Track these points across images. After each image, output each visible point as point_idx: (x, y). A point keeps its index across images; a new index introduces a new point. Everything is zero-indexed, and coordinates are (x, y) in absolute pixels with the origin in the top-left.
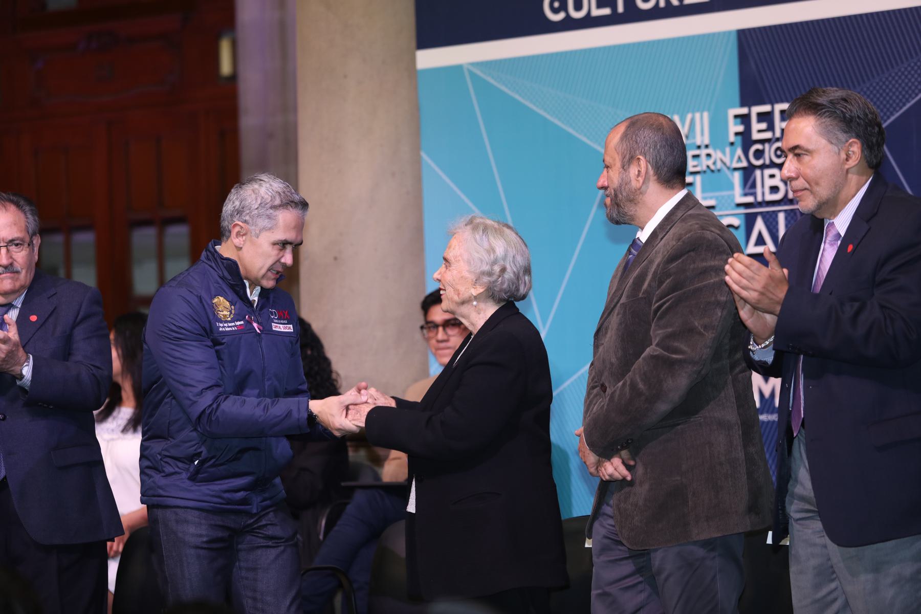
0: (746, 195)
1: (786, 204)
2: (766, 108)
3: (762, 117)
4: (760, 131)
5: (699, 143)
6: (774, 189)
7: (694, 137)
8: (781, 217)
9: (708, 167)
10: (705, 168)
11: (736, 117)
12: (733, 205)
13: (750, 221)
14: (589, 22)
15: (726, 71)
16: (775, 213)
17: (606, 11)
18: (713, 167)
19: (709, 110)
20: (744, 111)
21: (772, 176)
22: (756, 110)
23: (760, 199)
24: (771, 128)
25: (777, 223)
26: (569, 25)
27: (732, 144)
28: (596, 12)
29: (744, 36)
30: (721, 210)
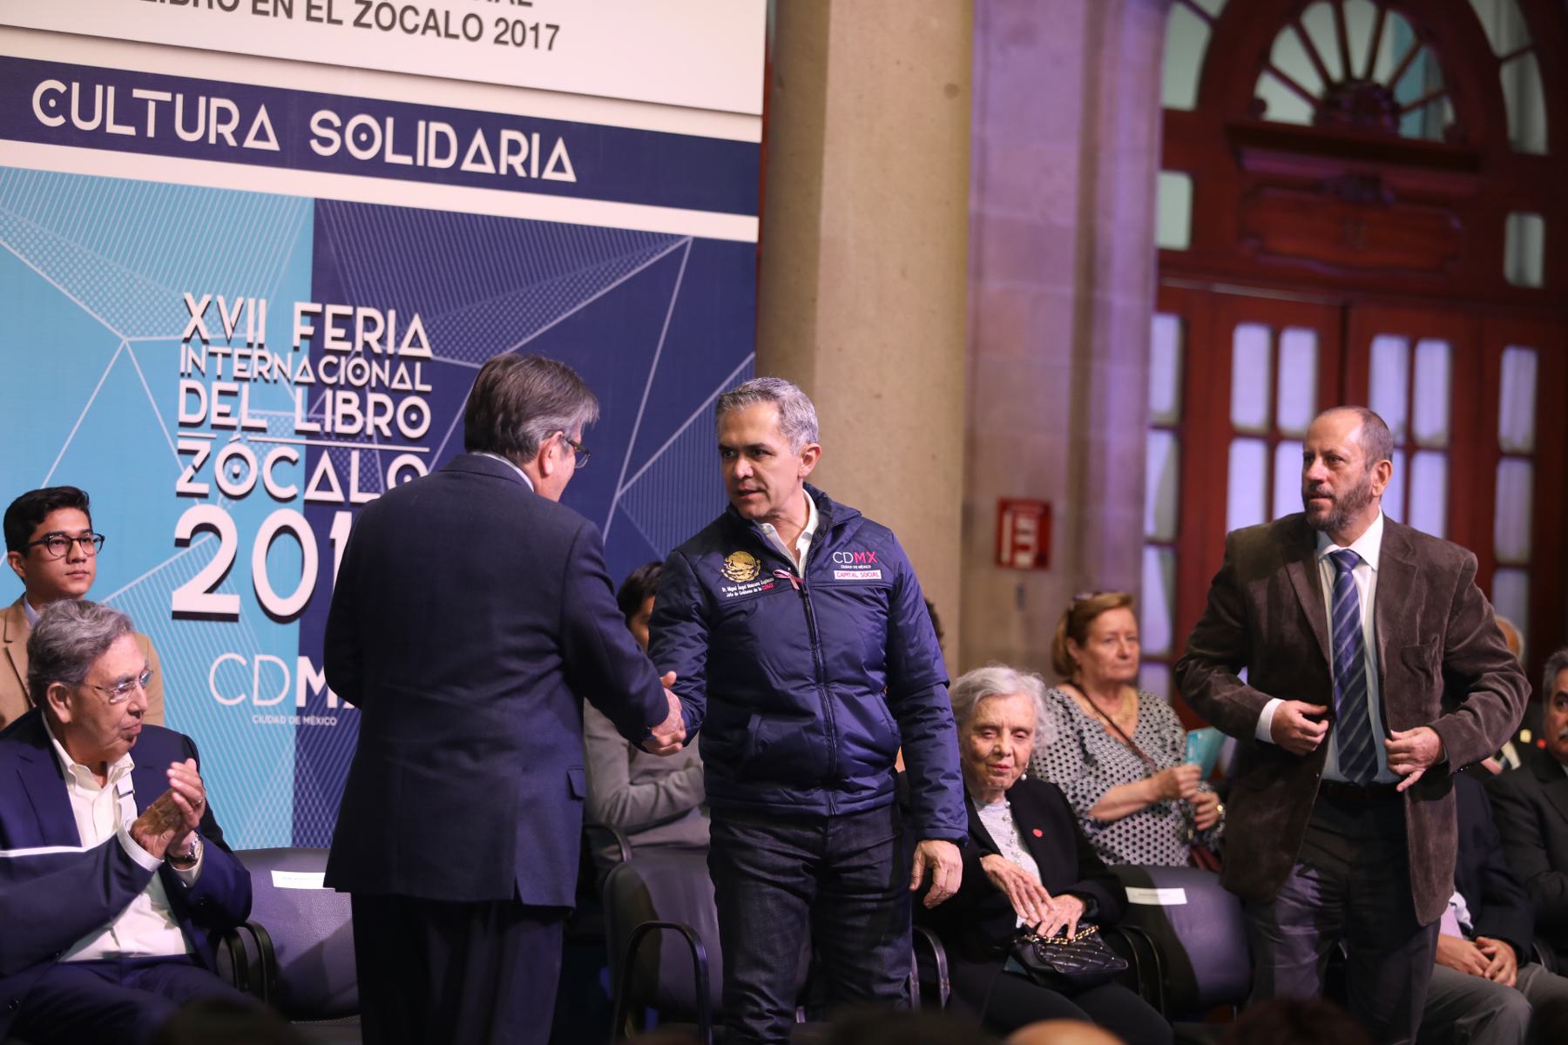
0: (309, 420)
1: (362, 441)
2: (347, 310)
3: (339, 320)
4: (334, 339)
5: (250, 340)
6: (348, 419)
7: (245, 331)
8: (355, 456)
10: (256, 375)
11: (304, 313)
12: (291, 431)
14: (100, 140)
15: (295, 252)
16: (348, 451)
17: (130, 131)
18: (267, 376)
19: (267, 298)
20: (317, 308)
22: (332, 309)
23: (328, 428)
24: (350, 337)
25: (349, 464)
26: (67, 136)
27: (296, 349)
28: (112, 128)
29: (325, 210)
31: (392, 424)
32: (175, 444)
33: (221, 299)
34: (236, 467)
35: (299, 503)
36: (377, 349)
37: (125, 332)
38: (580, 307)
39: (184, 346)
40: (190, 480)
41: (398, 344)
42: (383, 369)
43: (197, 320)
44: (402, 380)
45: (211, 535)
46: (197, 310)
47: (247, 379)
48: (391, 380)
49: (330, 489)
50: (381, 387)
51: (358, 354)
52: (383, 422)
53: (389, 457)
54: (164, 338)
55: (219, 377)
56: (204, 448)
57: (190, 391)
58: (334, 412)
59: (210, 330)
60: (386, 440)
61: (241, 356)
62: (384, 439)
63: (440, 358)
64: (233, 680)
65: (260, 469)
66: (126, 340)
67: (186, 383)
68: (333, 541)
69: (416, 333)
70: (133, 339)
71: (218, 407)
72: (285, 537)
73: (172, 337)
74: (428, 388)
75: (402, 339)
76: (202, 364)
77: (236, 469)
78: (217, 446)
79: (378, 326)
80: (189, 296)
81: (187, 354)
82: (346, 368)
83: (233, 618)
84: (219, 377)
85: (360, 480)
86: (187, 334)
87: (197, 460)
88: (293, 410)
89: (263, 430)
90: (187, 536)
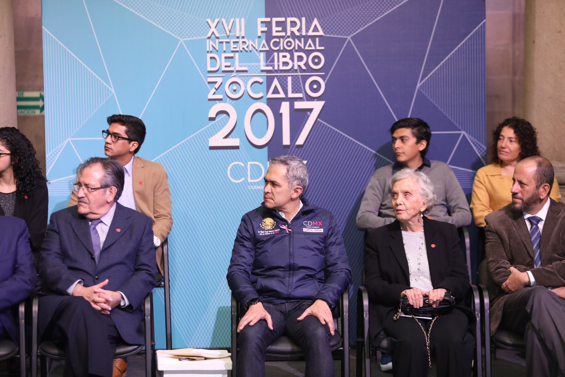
0: (267, 66)
1: (292, 72)
2: (283, 19)
3: (278, 24)
4: (277, 31)
5: (238, 35)
6: (285, 64)
7: (235, 32)
8: (290, 79)
9: (243, 48)
10: (241, 49)
11: (262, 22)
12: (259, 70)
13: (269, 81)
16: (286, 77)
18: (246, 49)
20: (268, 19)
21: (284, 57)
22: (275, 20)
23: (276, 68)
24: (284, 30)
27: (259, 37)
30: (251, 73)
31: (306, 64)
32: (207, 80)
33: (224, 20)
34: (235, 87)
35: (264, 99)
36: (297, 34)
37: (181, 37)
38: (395, 8)
39: (208, 40)
40: (214, 94)
41: (307, 31)
42: (300, 42)
43: (213, 29)
44: (310, 46)
45: (225, 115)
46: (213, 25)
47: (237, 51)
48: (305, 46)
49: (279, 93)
50: (300, 49)
51: (288, 37)
52: (302, 64)
53: (305, 78)
54: (199, 38)
55: (225, 52)
56: (219, 80)
58: (278, 62)
59: (219, 33)
60: (304, 71)
61: (234, 42)
62: (304, 71)
63: (328, 35)
64: (238, 172)
65: (246, 86)
66: (182, 40)
67: (209, 55)
68: (281, 114)
69: (316, 25)
70: (184, 40)
71: (224, 63)
72: (259, 114)
73: (202, 37)
74: (323, 48)
75: (309, 29)
77: (235, 88)
79: (297, 25)
81: (209, 45)
82: (283, 44)
83: (237, 148)
85: (292, 88)
86: (209, 35)
87: (217, 86)
88: (260, 62)
89: (246, 71)
90: (214, 116)
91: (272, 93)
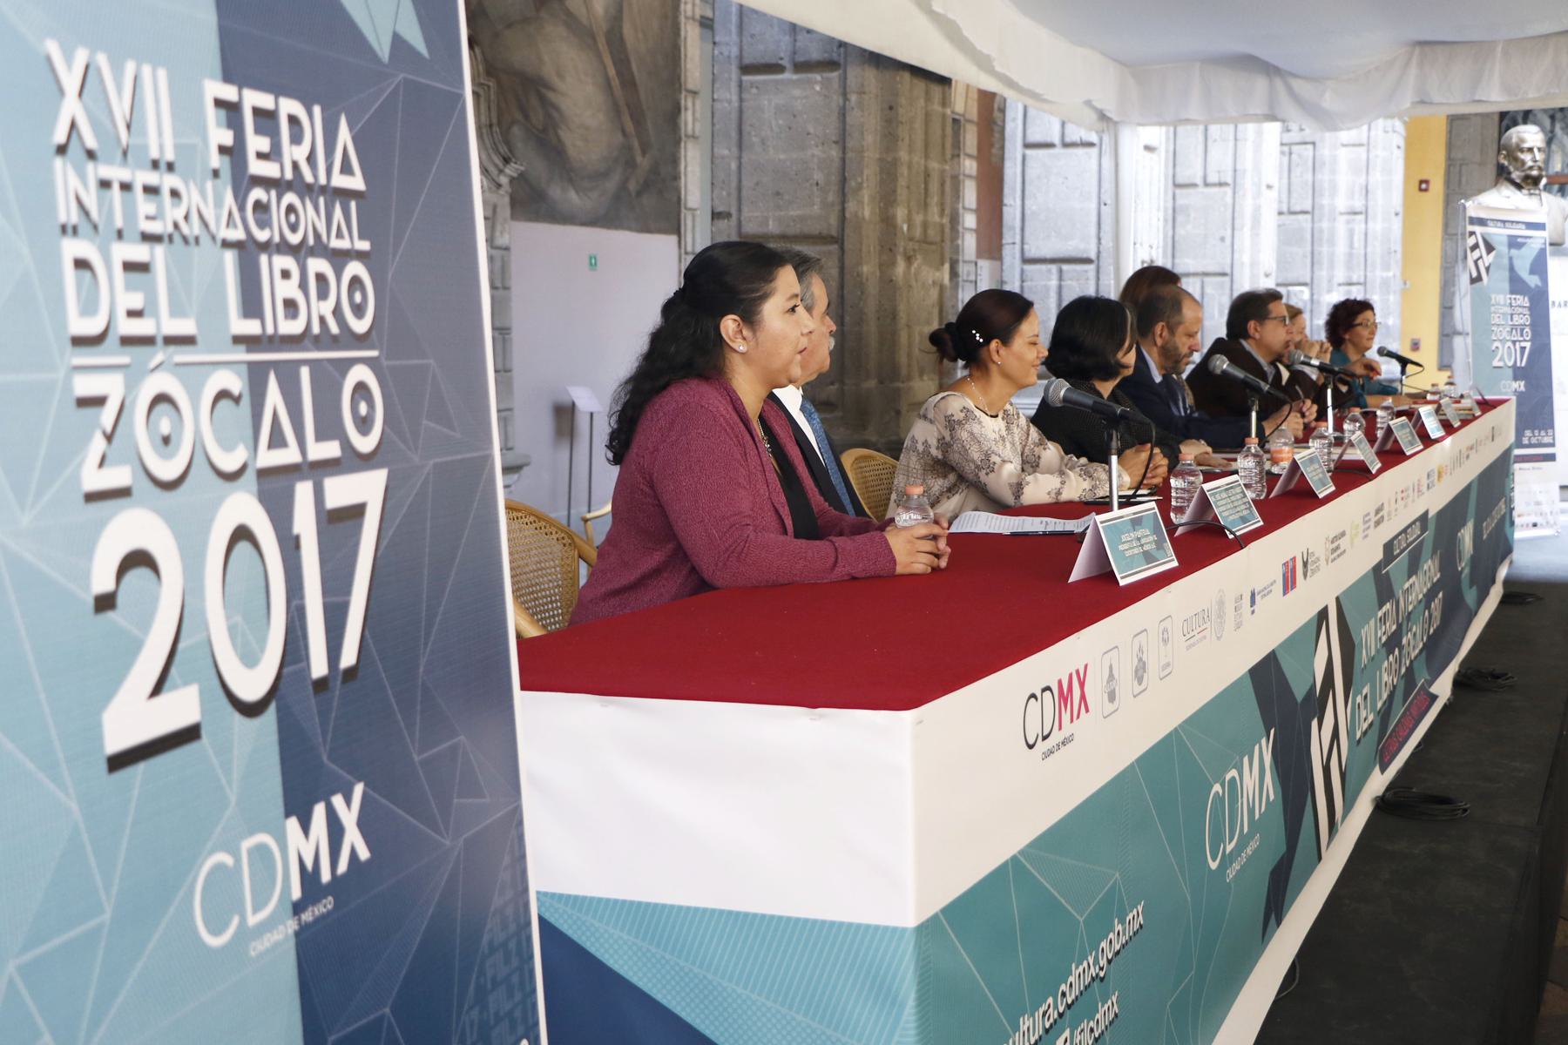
2: (265, 101)
3: (266, 119)
8: (305, 372)
11: (219, 103)
20: (229, 93)
22: (254, 99)
27: (216, 173)
31: (337, 312)
33: (102, 60)
39: (58, 162)
46: (71, 82)
52: (327, 308)
53: (345, 366)
55: (120, 234)
57: (81, 264)
67: (73, 248)
76: (91, 202)
77: (165, 427)
78: (133, 377)
80: (53, 48)
84: (120, 234)
86: (60, 136)
87: (107, 415)
89: (188, 341)
91: (271, 446)
